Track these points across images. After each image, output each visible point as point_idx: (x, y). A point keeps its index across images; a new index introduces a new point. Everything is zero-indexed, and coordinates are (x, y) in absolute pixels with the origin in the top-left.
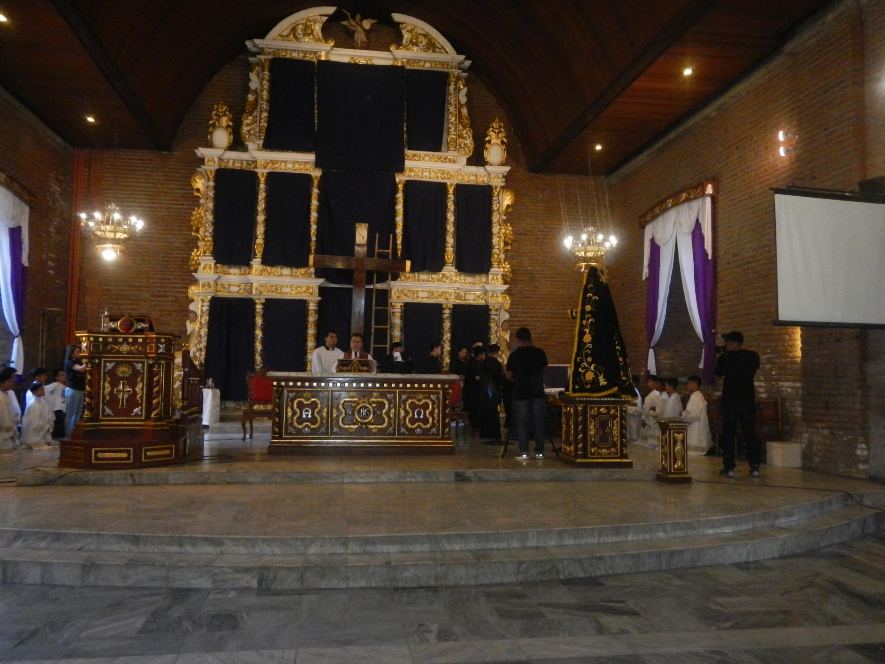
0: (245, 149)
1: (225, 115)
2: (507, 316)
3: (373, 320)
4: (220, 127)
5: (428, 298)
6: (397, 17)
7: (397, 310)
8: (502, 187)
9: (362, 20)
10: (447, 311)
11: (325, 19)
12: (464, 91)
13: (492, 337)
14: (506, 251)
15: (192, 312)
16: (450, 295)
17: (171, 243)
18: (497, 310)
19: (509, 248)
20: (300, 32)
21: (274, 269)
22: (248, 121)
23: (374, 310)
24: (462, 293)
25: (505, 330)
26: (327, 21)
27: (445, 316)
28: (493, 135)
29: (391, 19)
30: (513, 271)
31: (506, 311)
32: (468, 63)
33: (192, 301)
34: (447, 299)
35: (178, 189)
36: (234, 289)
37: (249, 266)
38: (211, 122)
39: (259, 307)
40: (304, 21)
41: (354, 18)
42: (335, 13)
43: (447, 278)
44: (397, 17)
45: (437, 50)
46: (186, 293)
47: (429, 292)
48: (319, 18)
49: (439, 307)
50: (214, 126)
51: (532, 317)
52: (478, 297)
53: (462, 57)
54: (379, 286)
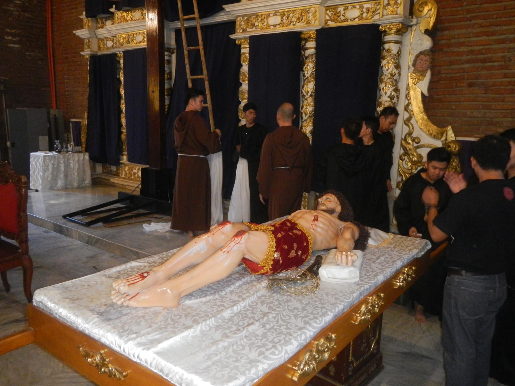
2: (427, 43)
3: (187, 66)
5: (282, 24)
7: (245, 50)
10: (311, 44)
13: (382, 86)
18: (399, 32)
21: (130, 16)
23: (186, 52)
24: (341, 9)
25: (420, 72)
27: (308, 53)
34: (308, 23)
36: (110, 44)
37: (113, 13)
39: (122, 61)
47: (283, 15)
49: (295, 40)
51: (503, 41)
52: (368, 10)
54: (221, 18)
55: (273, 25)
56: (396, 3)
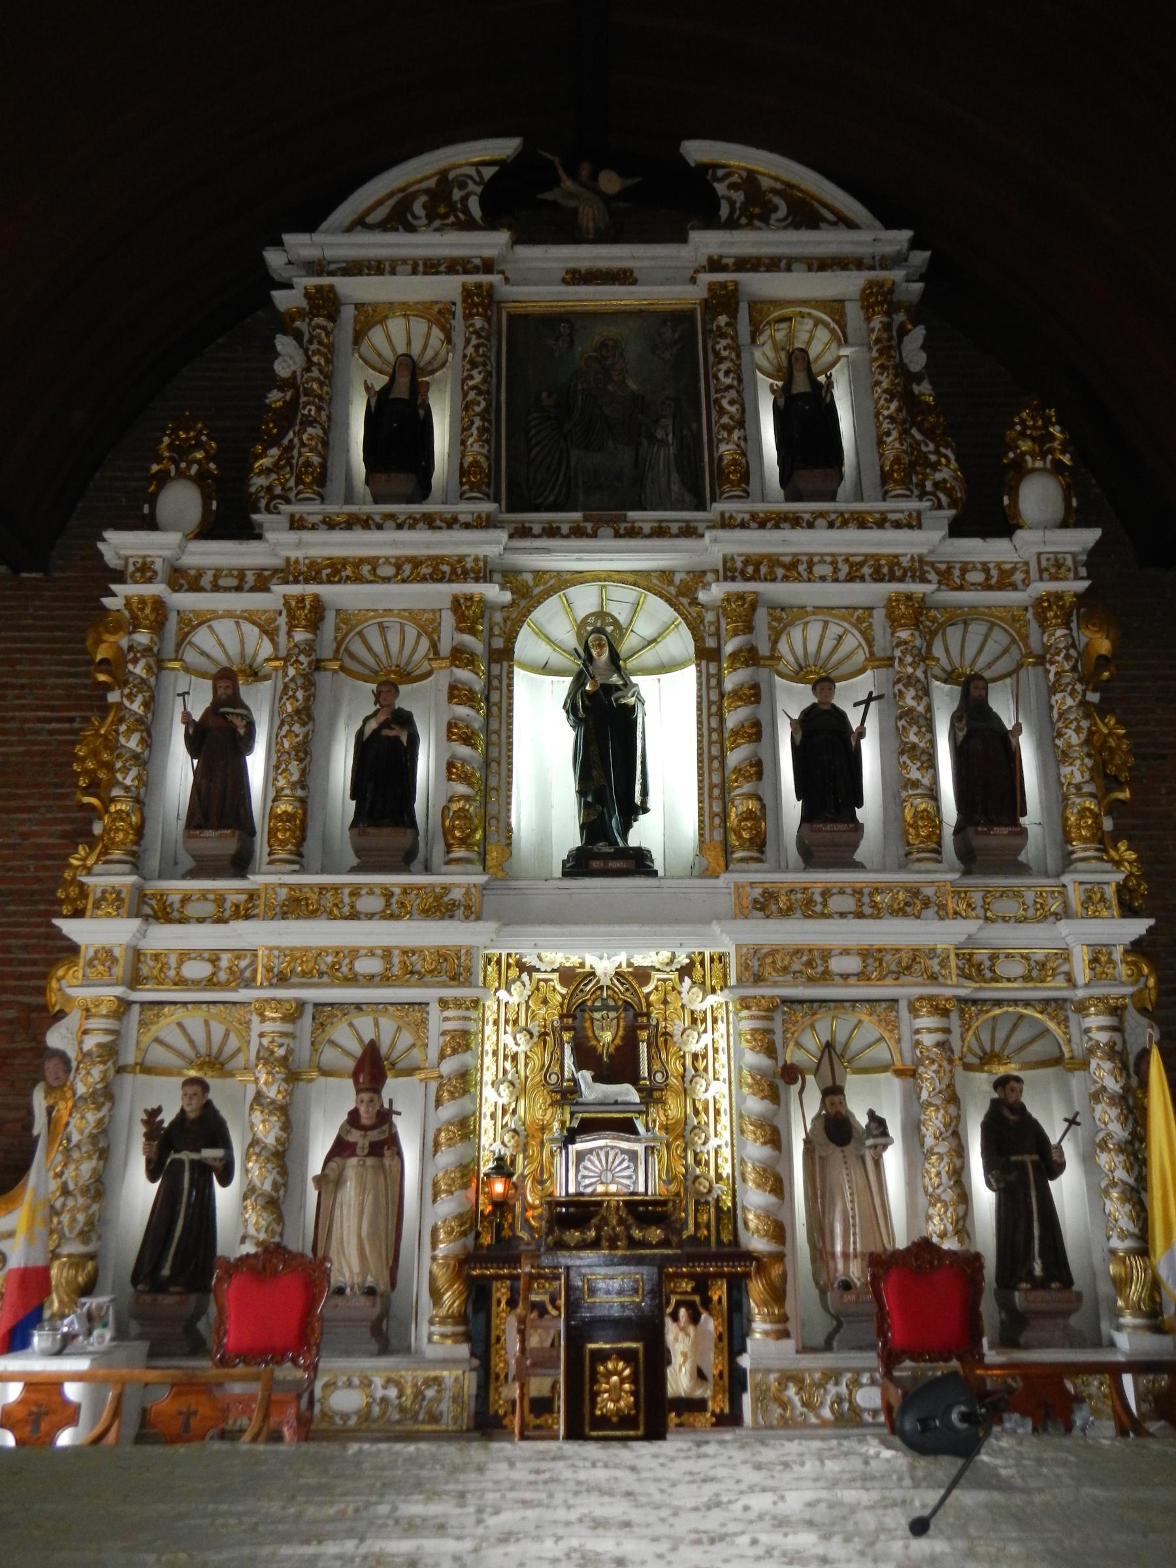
0: (251, 533)
1: (200, 446)
4: (181, 474)
6: (697, 151)
8: (1081, 598)
9: (594, 177)
11: (489, 172)
12: (917, 335)
14: (1114, 808)
15: (62, 1056)
16: (943, 964)
17: (25, 836)
19: (1125, 795)
20: (418, 207)
22: (266, 462)
24: (982, 955)
26: (494, 177)
28: (1025, 445)
29: (682, 160)
30: (1145, 876)
31: (1143, 1011)
32: (921, 257)
33: (61, 1015)
35: (60, 675)
38: (155, 468)
40: (431, 183)
41: (573, 175)
42: (521, 157)
43: (926, 904)
44: (697, 151)
45: (822, 225)
46: (42, 991)
48: (471, 171)
50: (163, 479)
53: (906, 235)
55: (841, 975)
56: (1110, 961)
